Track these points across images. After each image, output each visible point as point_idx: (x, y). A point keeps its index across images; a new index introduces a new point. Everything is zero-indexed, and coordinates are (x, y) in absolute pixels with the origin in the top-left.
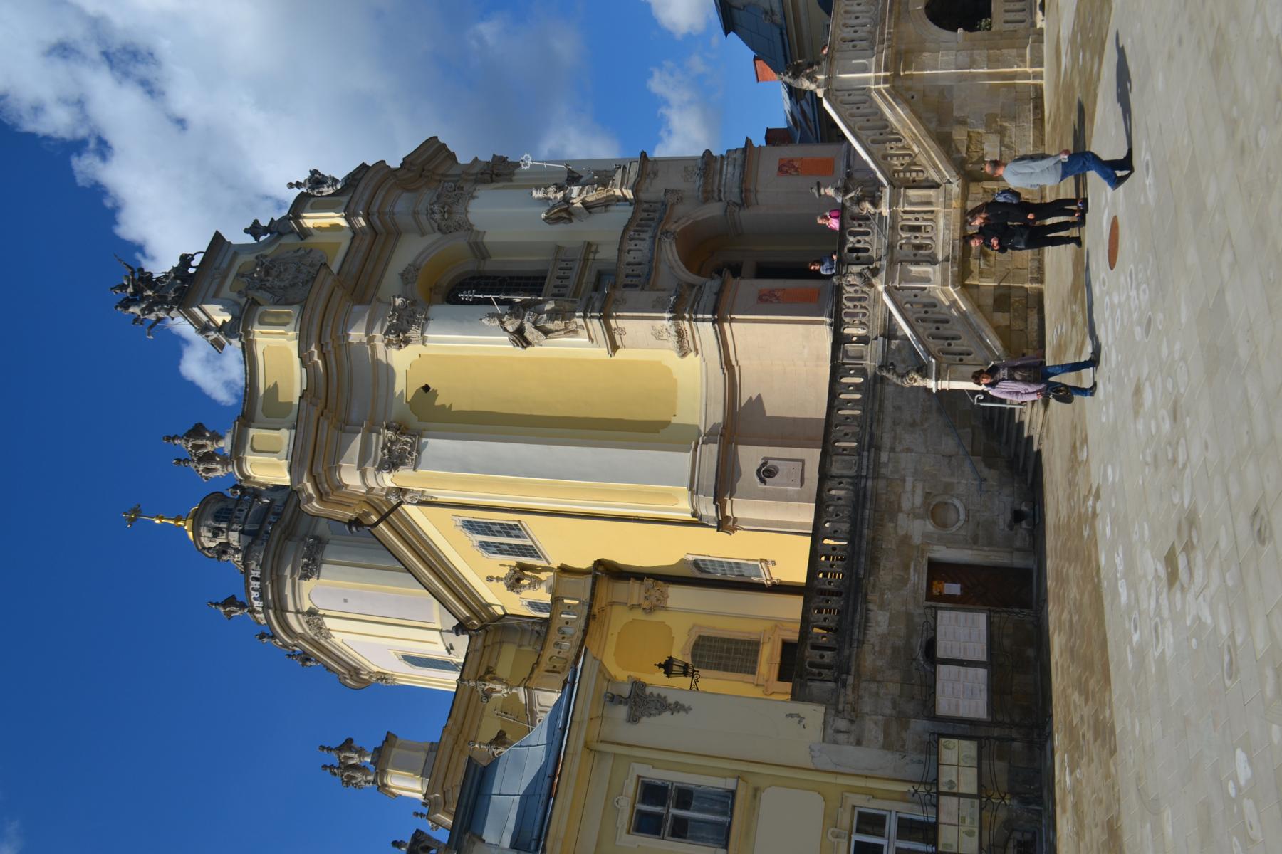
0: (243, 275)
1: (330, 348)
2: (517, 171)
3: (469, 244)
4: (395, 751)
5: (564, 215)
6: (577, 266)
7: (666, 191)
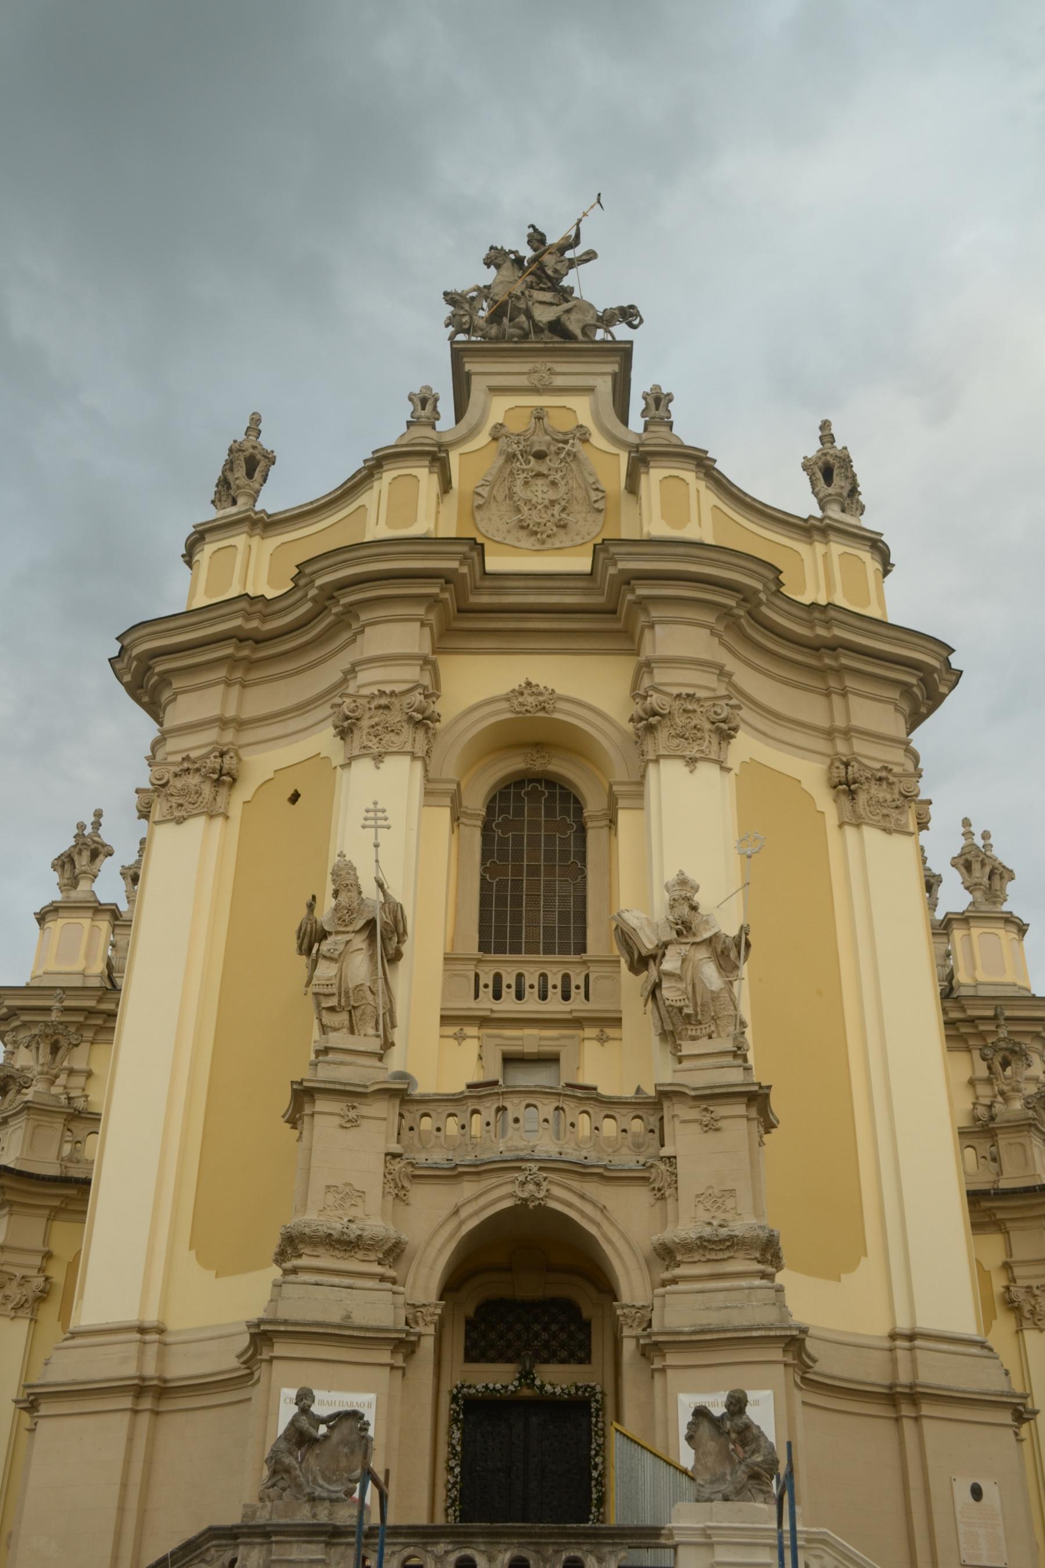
0: (539, 418)
1: (335, 610)
2: (871, 834)
3: (611, 786)
4: (86, 923)
5: (636, 957)
6: (577, 1004)
7: (671, 1160)
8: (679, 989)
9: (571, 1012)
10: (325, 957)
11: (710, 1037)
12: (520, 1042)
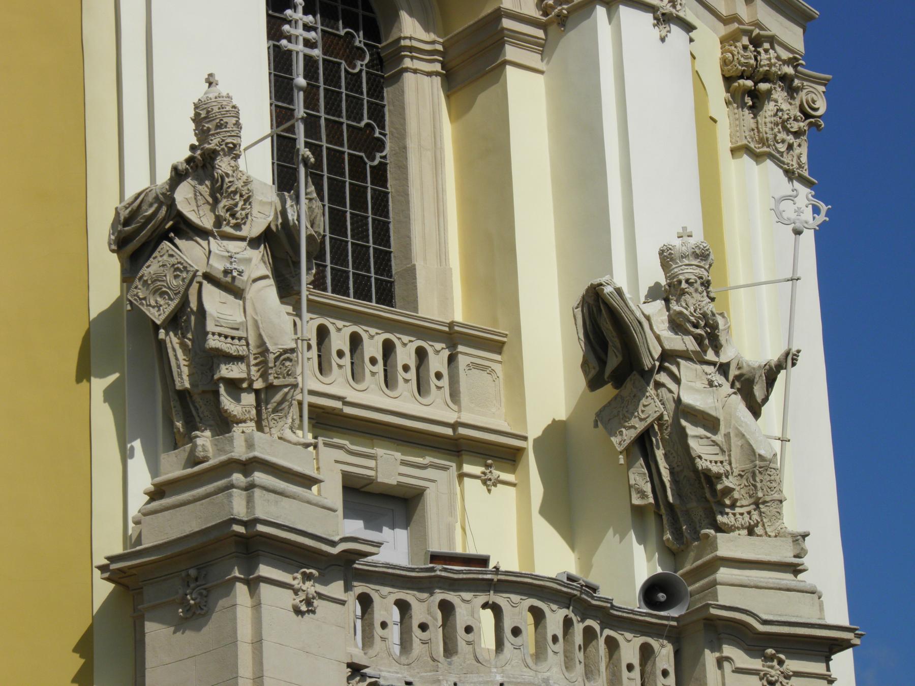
5: (614, 360)
8: (715, 443)
9: (454, 426)
10: (208, 277)
11: (751, 532)
12: (372, 463)
